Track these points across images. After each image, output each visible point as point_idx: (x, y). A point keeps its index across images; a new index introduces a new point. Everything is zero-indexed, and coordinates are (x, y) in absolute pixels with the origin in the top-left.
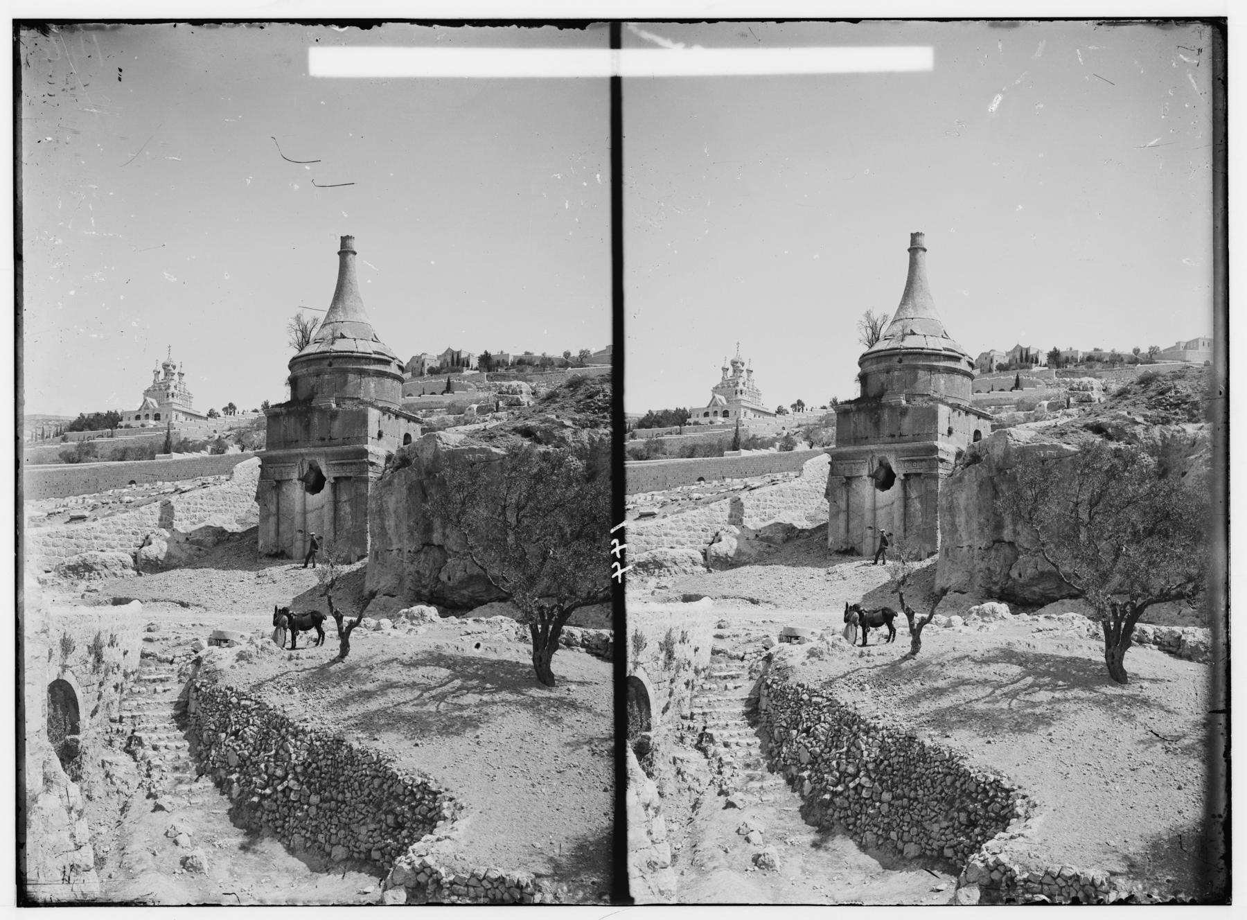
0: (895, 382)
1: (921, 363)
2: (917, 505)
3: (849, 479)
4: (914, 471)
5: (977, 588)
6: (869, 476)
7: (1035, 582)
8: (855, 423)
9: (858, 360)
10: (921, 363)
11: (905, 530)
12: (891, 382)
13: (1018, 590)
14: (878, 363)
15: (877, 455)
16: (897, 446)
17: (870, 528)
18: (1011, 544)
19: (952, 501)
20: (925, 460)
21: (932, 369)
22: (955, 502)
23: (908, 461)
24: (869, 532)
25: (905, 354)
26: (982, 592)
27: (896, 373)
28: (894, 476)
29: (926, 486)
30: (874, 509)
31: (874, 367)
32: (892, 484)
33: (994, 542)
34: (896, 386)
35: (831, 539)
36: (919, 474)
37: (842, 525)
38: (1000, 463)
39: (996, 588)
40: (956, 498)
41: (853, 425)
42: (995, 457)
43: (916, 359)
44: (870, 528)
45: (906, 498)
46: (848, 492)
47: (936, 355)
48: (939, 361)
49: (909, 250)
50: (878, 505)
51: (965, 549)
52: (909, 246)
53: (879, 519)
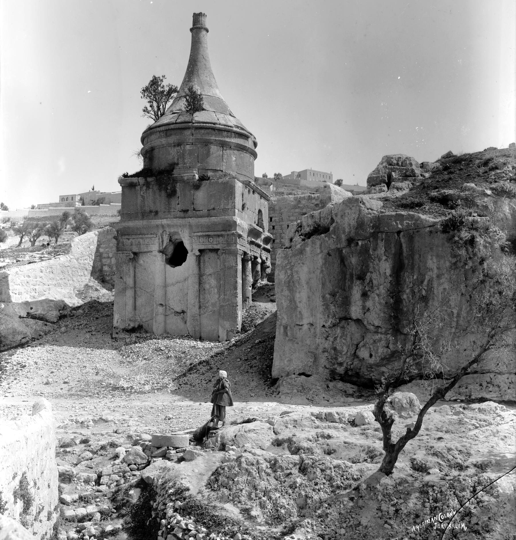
0: (187, 156)
1: (213, 138)
2: (211, 282)
3: (135, 254)
4: (210, 247)
5: (321, 369)
6: (160, 251)
7: (385, 362)
8: (142, 196)
9: (141, 135)
10: (213, 138)
11: (200, 307)
12: (182, 156)
13: (364, 371)
14: (167, 136)
15: (167, 230)
16: (193, 221)
17: (161, 305)
18: (358, 321)
19: (292, 275)
20: (222, 236)
21: (223, 145)
22: (295, 276)
23: (203, 236)
24: (161, 309)
25: (197, 128)
26: (326, 373)
27: (188, 147)
28: (186, 252)
29: (224, 261)
30: (165, 286)
31: (164, 141)
32: (184, 260)
33: (341, 319)
34: (188, 160)
35: (116, 317)
36: (216, 251)
37: (130, 302)
38: (352, 234)
39: (341, 370)
40: (297, 272)
41: (140, 199)
42: (346, 226)
43: (208, 134)
44: (161, 305)
45: (200, 276)
46: (135, 268)
47: (228, 131)
48: (231, 137)
49: (191, 30)
50: (169, 281)
51: (306, 327)
52: (191, 26)
53: (170, 296)
